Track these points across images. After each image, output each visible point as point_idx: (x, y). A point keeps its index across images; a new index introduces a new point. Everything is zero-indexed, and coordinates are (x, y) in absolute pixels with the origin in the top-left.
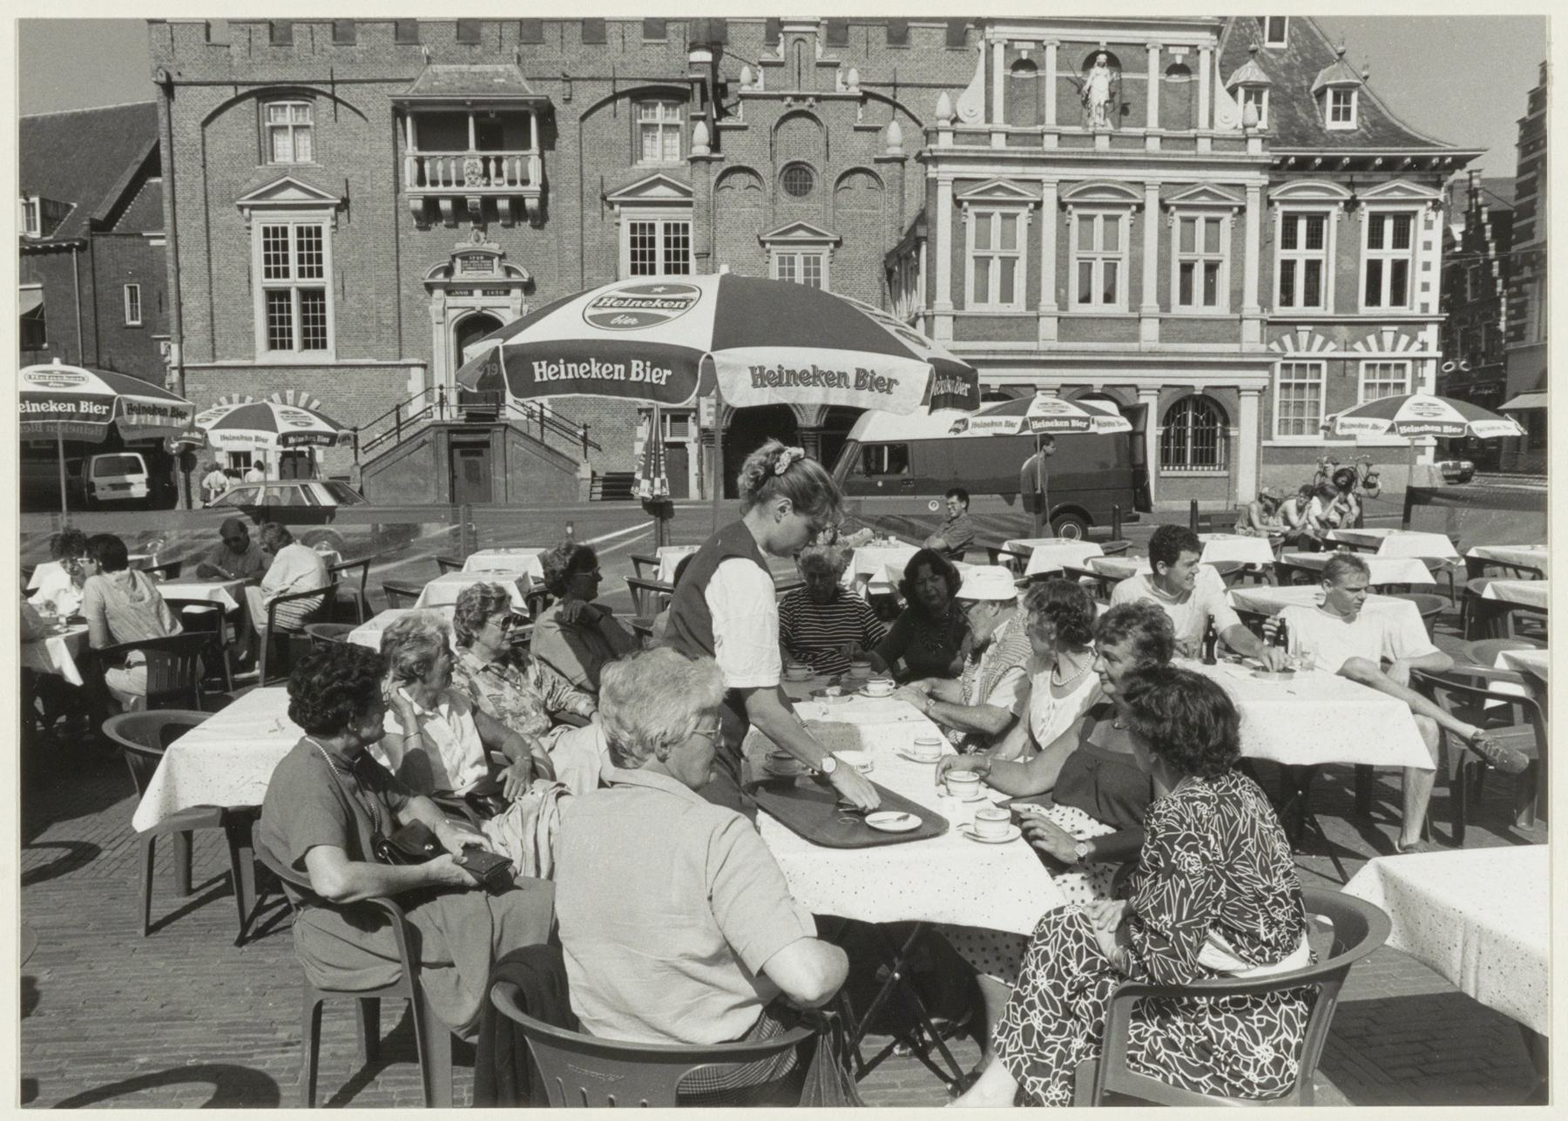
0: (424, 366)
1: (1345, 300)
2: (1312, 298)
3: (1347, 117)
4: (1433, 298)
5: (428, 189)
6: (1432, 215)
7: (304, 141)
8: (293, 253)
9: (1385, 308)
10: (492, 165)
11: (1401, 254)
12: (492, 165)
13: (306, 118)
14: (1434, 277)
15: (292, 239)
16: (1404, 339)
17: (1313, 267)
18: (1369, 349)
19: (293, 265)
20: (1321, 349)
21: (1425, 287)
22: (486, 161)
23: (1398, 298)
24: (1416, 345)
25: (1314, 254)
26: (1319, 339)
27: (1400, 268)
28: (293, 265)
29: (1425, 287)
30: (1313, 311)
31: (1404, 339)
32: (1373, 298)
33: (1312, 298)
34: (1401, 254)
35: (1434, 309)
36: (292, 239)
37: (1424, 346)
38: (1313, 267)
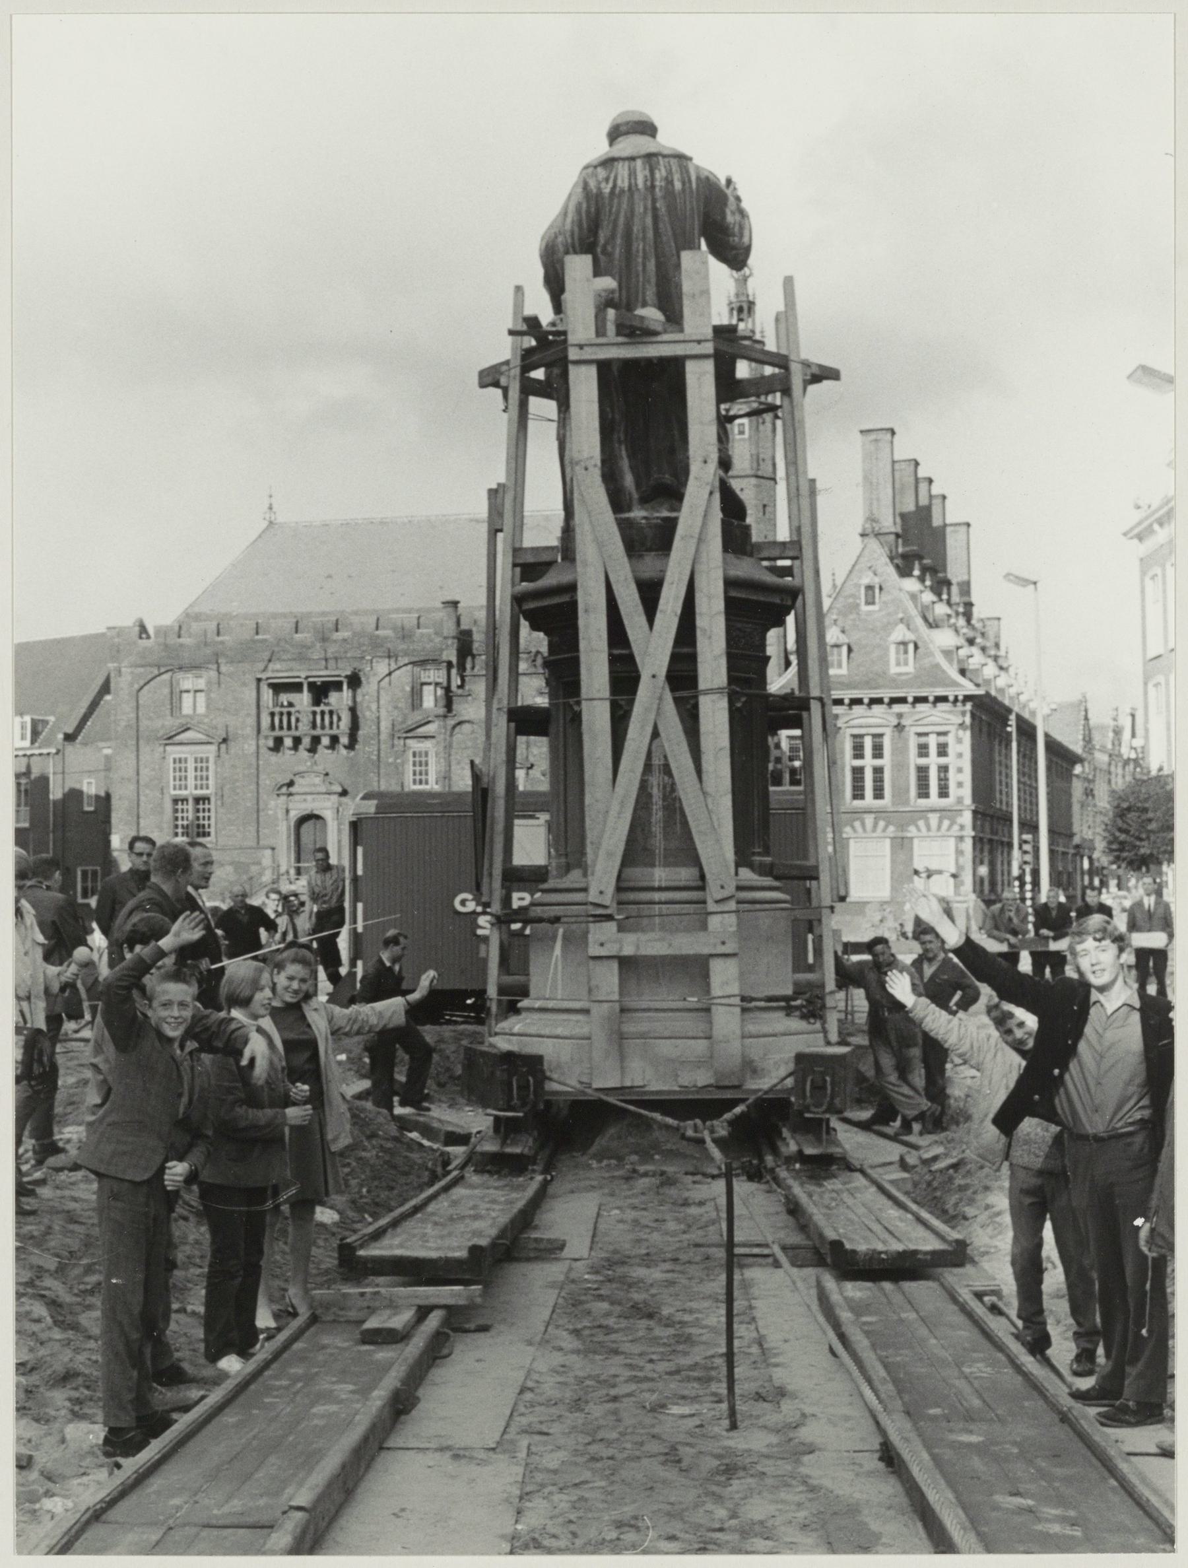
0: (273, 849)
1: (900, 793)
2: (879, 793)
3: (906, 664)
4: (967, 792)
5: (277, 733)
6: (961, 733)
7: (201, 698)
8: (191, 774)
9: (934, 799)
10: (318, 718)
11: (943, 761)
12: (318, 718)
13: (201, 683)
14: (967, 777)
15: (191, 765)
16: (946, 823)
17: (878, 771)
18: (919, 830)
19: (191, 782)
20: (884, 830)
21: (960, 785)
22: (314, 713)
23: (944, 793)
24: (956, 827)
25: (878, 762)
26: (882, 824)
27: (944, 769)
28: (191, 782)
29: (960, 785)
30: (879, 802)
31: (946, 823)
32: (923, 792)
33: (879, 793)
34: (943, 761)
35: (968, 800)
36: (191, 765)
37: (962, 827)
38: (878, 771)
